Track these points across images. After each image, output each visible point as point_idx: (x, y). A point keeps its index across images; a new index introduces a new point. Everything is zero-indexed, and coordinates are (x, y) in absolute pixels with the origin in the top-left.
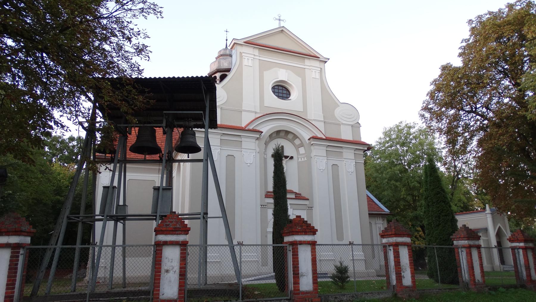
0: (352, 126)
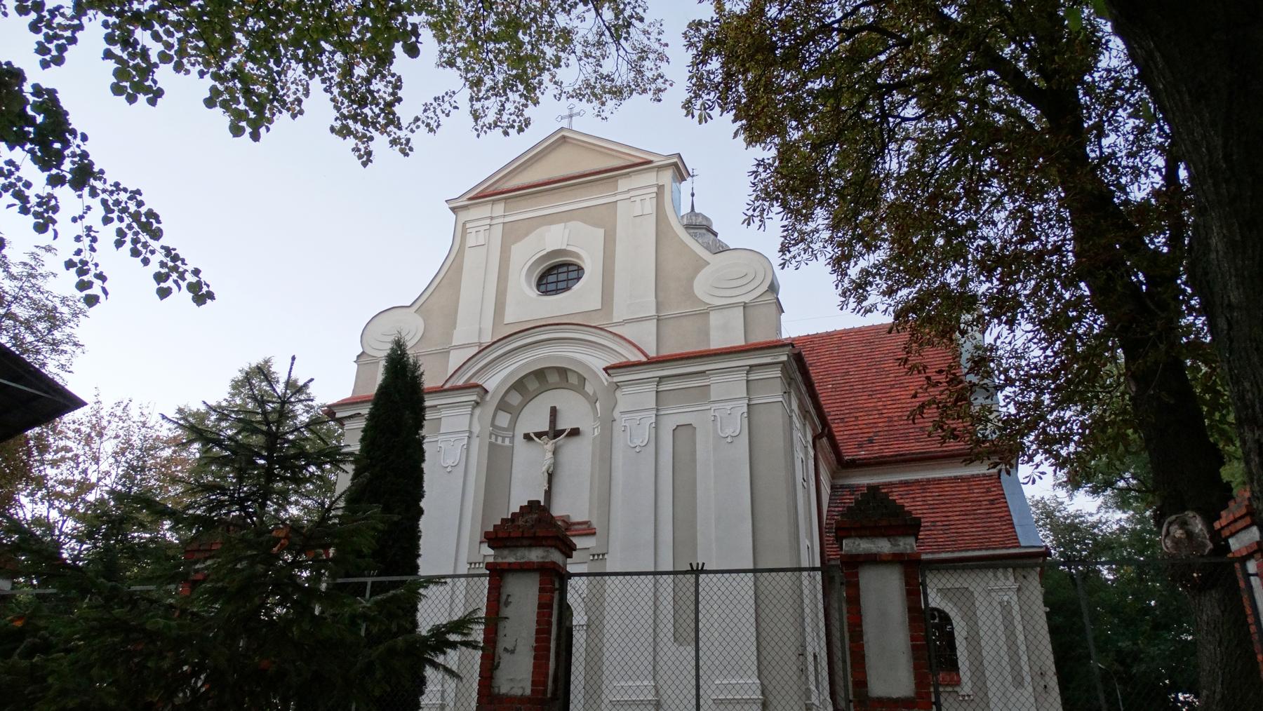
0: (745, 306)
